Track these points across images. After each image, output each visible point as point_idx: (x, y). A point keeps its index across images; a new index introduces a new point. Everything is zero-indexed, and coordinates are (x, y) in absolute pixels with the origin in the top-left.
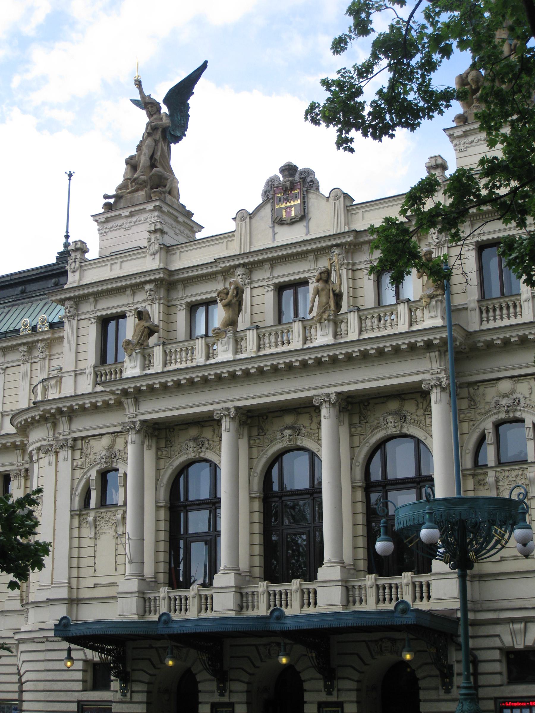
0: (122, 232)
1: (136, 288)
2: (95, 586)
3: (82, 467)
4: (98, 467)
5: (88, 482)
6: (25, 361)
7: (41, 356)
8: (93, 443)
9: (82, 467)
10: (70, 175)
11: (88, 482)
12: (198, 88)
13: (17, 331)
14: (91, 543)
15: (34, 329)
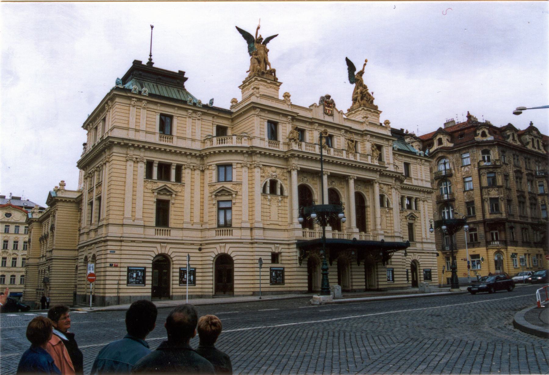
0: (265, 88)
1: (286, 116)
2: (271, 224)
3: (264, 177)
4: (271, 178)
5: (266, 183)
6: (190, 117)
7: (199, 118)
8: (267, 168)
9: (264, 177)
10: (152, 27)
11: (266, 183)
12: (271, 41)
13: (185, 102)
14: (268, 207)
15: (195, 104)
